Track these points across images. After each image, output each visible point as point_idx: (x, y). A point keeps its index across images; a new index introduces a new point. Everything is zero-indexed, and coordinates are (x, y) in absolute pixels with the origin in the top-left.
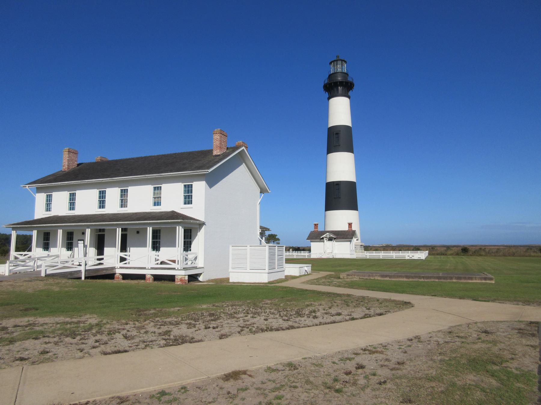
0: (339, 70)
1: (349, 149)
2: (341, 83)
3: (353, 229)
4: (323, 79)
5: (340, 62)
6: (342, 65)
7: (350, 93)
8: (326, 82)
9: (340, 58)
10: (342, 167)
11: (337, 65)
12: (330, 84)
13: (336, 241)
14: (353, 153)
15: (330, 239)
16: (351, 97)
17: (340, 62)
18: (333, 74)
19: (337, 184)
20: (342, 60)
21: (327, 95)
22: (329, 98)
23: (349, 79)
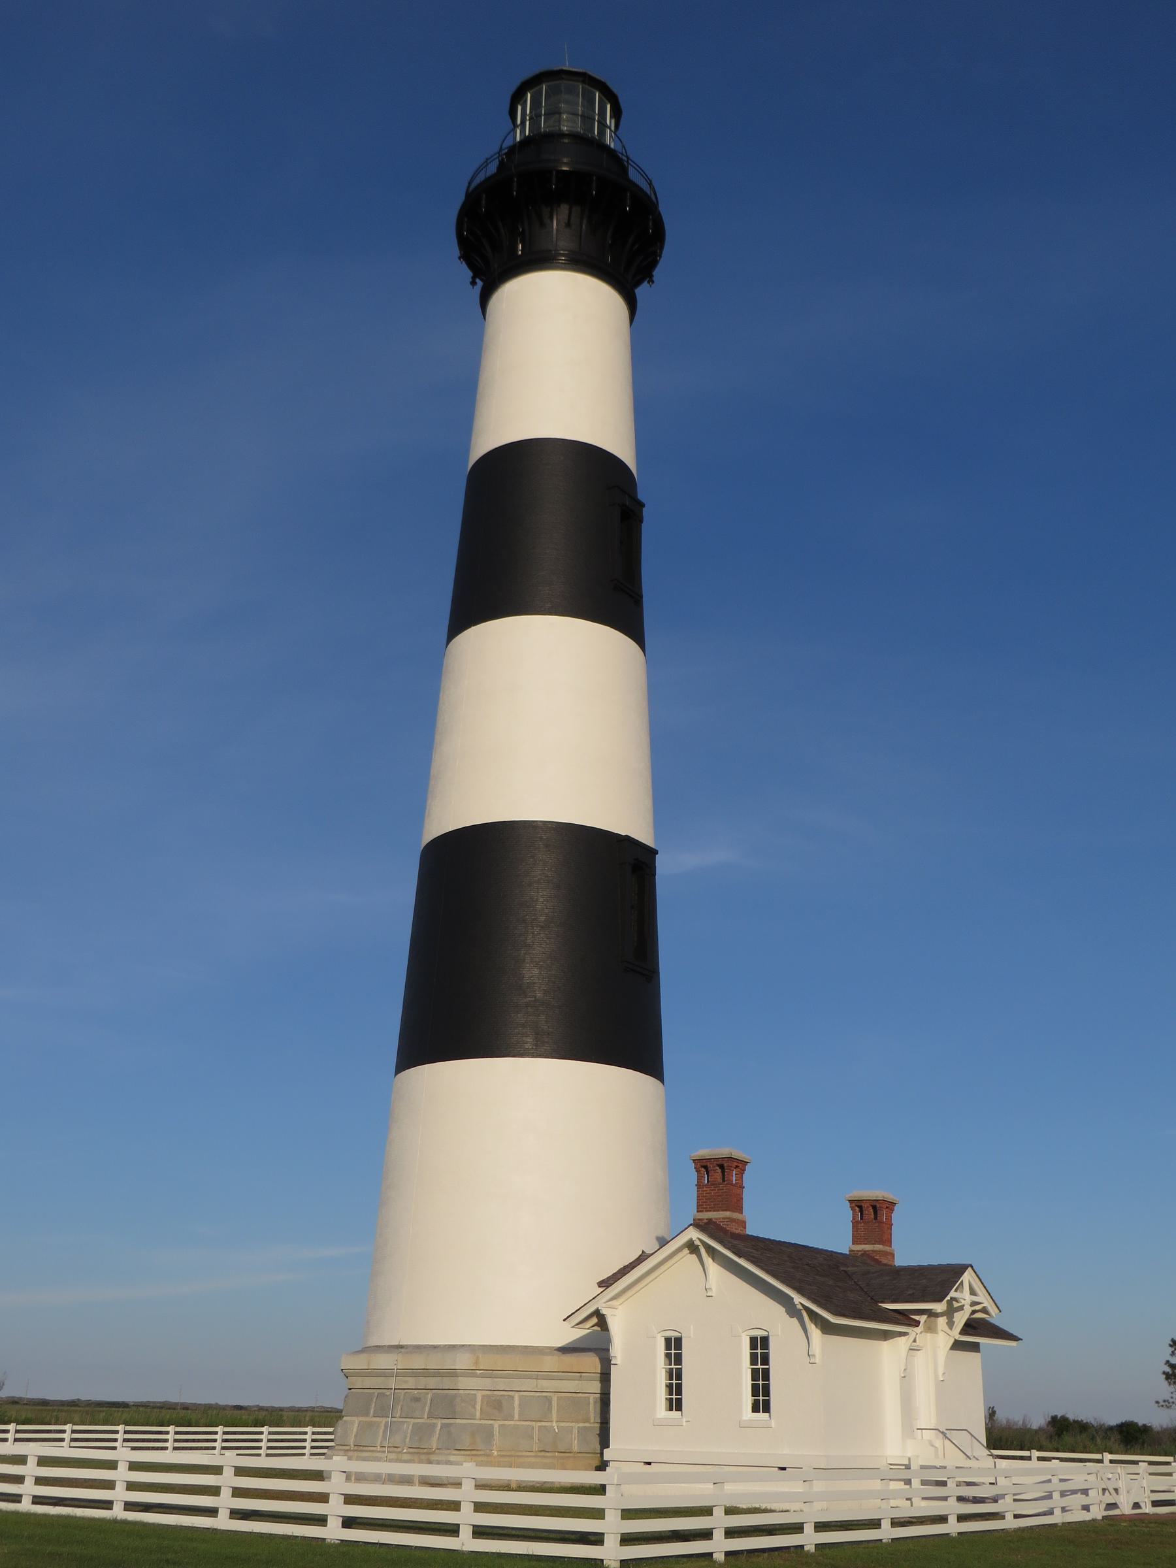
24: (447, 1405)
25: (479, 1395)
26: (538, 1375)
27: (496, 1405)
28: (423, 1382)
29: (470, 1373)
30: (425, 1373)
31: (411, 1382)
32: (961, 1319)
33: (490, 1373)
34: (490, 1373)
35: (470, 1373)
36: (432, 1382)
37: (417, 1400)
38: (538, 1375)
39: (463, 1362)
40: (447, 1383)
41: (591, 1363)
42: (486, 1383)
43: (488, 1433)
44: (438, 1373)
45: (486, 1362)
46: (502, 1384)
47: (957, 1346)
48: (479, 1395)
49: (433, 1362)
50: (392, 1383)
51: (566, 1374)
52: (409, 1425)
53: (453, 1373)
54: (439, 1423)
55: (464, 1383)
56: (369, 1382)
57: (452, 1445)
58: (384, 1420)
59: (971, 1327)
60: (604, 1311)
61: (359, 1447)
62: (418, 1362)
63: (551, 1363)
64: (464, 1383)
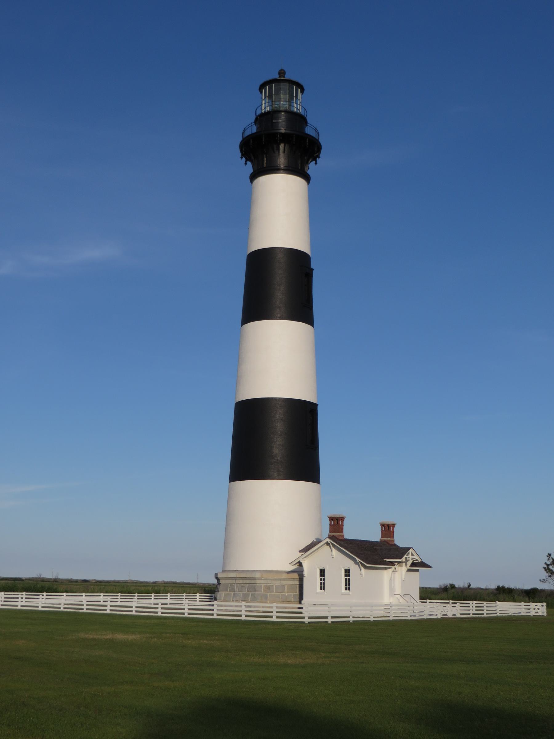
0: (283, 104)
2: (285, 138)
4: (244, 123)
11: (277, 93)
18: (266, 113)
20: (292, 83)
21: (249, 168)
22: (254, 177)
23: (309, 131)
24: (253, 588)
25: (263, 585)
26: (281, 579)
27: (268, 588)
28: (245, 581)
29: (260, 579)
30: (246, 579)
31: (241, 581)
32: (409, 563)
33: (266, 579)
34: (266, 579)
35: (260, 579)
36: (248, 581)
37: (243, 586)
38: (281, 579)
39: (258, 575)
40: (253, 582)
41: (296, 576)
42: (265, 582)
43: (266, 597)
44: (250, 579)
45: (265, 576)
46: (270, 582)
47: (409, 570)
48: (263, 585)
49: (248, 576)
50: (236, 581)
51: (289, 579)
52: (241, 594)
53: (255, 579)
54: (251, 593)
55: (258, 582)
56: (227, 581)
57: (254, 599)
58: (233, 593)
59: (414, 564)
60: (301, 561)
61: (225, 601)
62: (243, 575)
63: (285, 576)
64: (258, 582)
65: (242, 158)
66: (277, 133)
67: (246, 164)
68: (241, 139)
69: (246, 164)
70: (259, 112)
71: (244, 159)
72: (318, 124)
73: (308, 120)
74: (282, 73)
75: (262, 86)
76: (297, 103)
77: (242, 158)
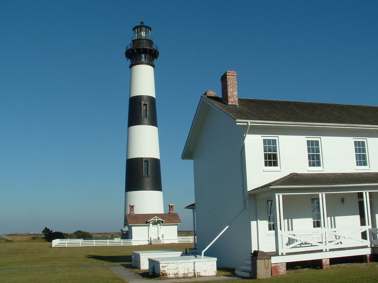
1: (153, 122)
3: (175, 211)
5: (144, 29)
6: (146, 33)
7: (155, 62)
8: (129, 47)
9: (144, 24)
10: (146, 142)
11: (141, 31)
12: (132, 50)
13: (163, 225)
14: (157, 127)
15: (155, 223)
16: (156, 66)
17: (144, 29)
19: (139, 161)
20: (146, 27)
21: (129, 62)
22: (131, 66)
23: (154, 47)
65: (126, 58)
66: (141, 48)
67: (128, 60)
68: (125, 51)
69: (128, 60)
70: (133, 40)
71: (127, 58)
72: (158, 45)
73: (153, 42)
74: (142, 23)
75: (134, 29)
76: (148, 35)
77: (126, 58)
